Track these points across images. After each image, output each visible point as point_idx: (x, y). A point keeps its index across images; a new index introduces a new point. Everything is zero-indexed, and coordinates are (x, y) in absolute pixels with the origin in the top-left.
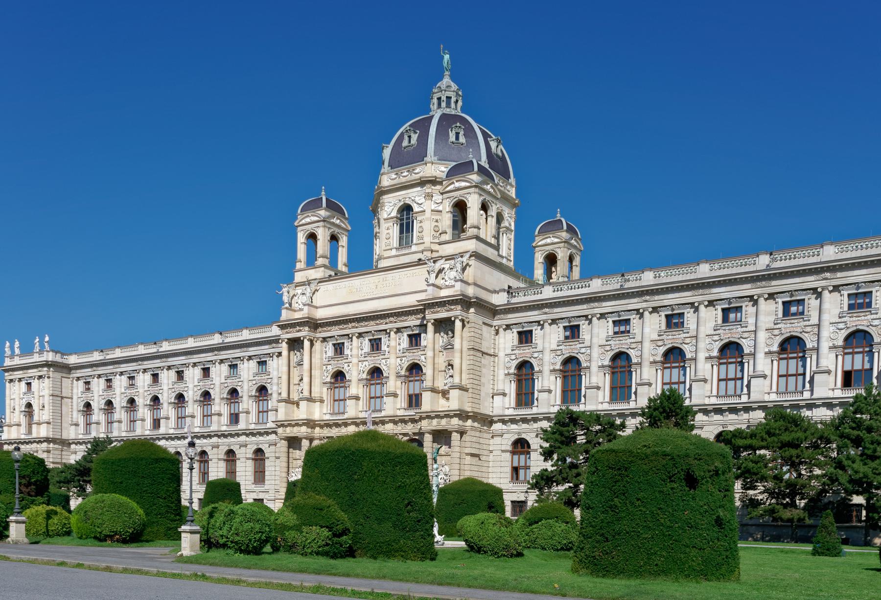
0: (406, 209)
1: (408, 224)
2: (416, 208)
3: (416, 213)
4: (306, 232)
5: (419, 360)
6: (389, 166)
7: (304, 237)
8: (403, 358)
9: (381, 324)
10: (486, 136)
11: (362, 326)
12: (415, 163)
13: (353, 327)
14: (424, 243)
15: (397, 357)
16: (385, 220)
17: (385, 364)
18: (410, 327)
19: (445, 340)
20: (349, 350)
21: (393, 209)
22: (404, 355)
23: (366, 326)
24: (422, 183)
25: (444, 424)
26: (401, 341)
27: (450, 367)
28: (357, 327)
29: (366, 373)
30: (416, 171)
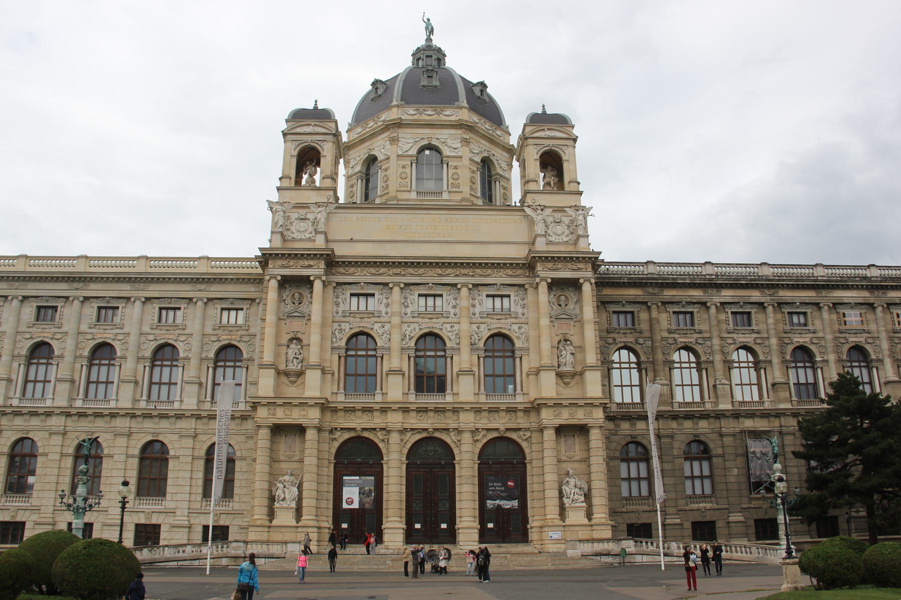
2: (446, 152)
3: (448, 157)
4: (301, 144)
6: (401, 100)
8: (482, 326)
11: (412, 275)
14: (461, 192)
15: (471, 323)
16: (398, 156)
17: (449, 329)
18: (496, 284)
19: (555, 308)
21: (411, 147)
22: (483, 320)
23: (419, 275)
24: (460, 125)
25: (580, 417)
26: (476, 302)
28: (404, 275)
30: (445, 113)
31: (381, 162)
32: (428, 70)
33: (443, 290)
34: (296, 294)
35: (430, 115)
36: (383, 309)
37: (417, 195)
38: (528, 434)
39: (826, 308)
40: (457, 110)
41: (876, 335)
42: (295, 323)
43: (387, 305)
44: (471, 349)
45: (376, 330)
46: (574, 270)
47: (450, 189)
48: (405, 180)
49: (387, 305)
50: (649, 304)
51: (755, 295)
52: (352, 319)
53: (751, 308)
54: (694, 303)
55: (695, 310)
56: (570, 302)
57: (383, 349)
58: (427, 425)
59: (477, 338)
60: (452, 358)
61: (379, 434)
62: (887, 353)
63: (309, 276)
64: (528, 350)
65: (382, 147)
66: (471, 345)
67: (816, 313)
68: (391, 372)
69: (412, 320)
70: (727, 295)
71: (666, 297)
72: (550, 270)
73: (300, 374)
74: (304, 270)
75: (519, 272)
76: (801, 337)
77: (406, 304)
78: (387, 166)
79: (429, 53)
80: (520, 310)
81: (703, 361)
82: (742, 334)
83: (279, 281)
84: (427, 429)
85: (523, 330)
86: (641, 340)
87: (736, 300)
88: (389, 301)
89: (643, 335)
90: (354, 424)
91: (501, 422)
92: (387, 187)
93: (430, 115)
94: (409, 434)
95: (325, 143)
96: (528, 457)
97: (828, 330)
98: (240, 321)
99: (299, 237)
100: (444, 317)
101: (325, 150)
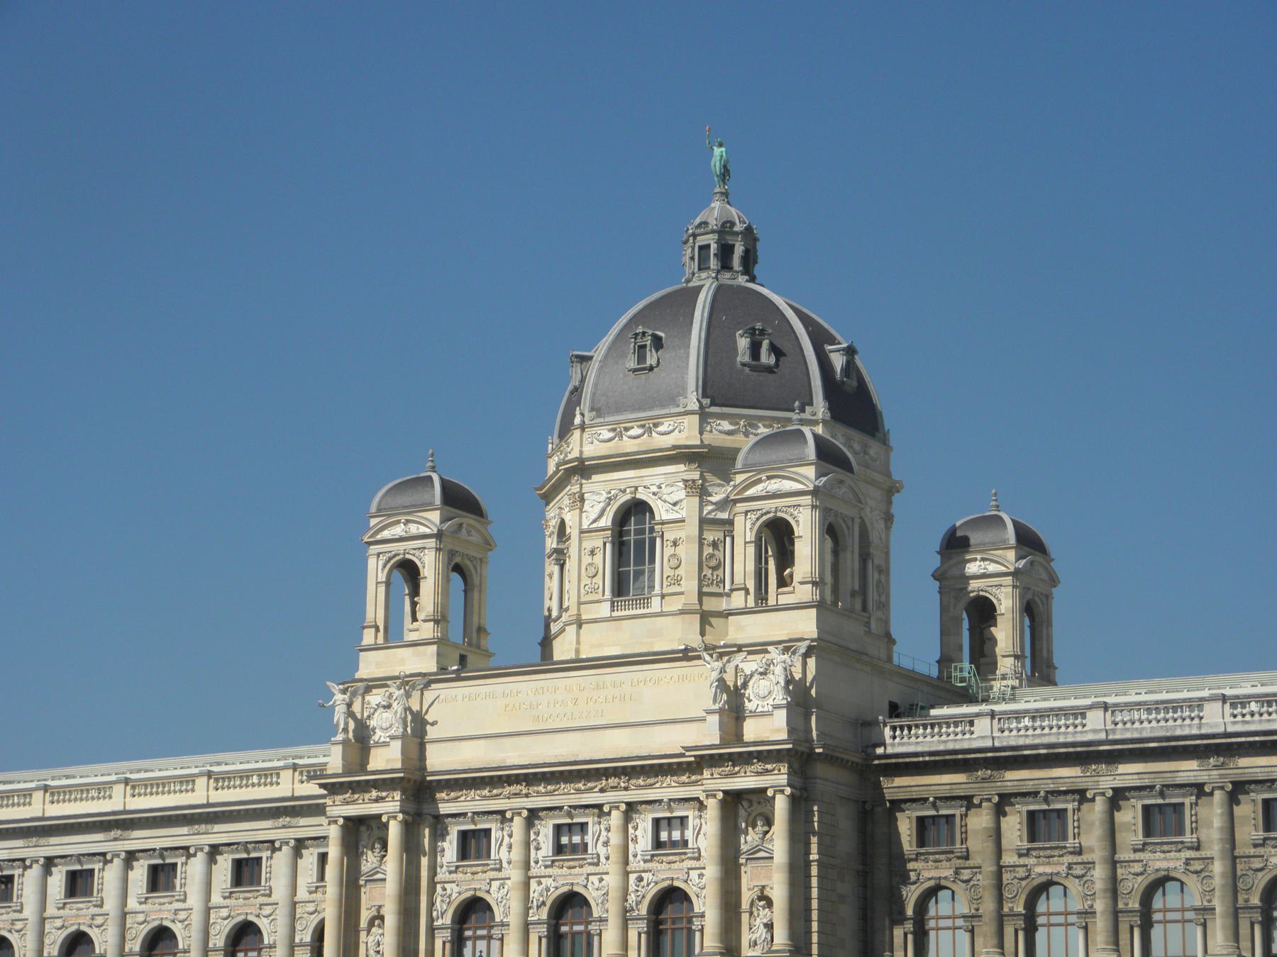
0: (634, 511)
1: (640, 545)
2: (662, 512)
3: (663, 523)
4: (390, 559)
5: (686, 881)
9: (590, 790)
10: (820, 338)
13: (517, 795)
14: (682, 593)
20: (504, 849)
26: (639, 833)
27: (762, 903)
28: (527, 796)
32: (637, 334)
35: (635, 438)
37: (612, 606)
40: (679, 419)
43: (510, 847)
46: (759, 774)
47: (665, 591)
48: (594, 580)
51: (1188, 770)
52: (459, 876)
53: (1184, 796)
55: (1070, 806)
59: (634, 899)
63: (379, 816)
66: (625, 911)
69: (543, 871)
70: (1129, 773)
71: (1009, 784)
79: (702, 240)
82: (1164, 852)
86: (966, 871)
87: (1146, 782)
89: (971, 863)
93: (635, 438)
95: (426, 551)
100: (590, 864)
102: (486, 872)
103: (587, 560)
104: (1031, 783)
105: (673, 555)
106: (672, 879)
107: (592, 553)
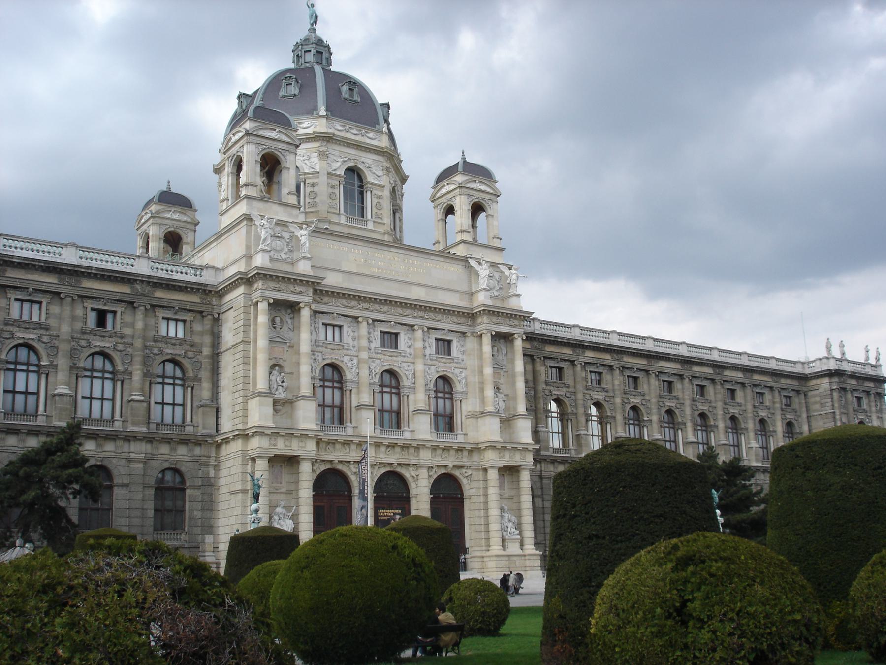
0: (354, 172)
2: (370, 178)
3: (373, 184)
4: (265, 149)
7: (261, 155)
8: (433, 367)
12: (352, 121)
14: (384, 224)
15: (425, 364)
16: (328, 173)
17: (406, 369)
18: (444, 329)
23: (384, 313)
28: (372, 311)
29: (378, 376)
30: (368, 135)
31: (305, 174)
32: (351, 82)
33: (401, 330)
34: (278, 320)
35: (356, 135)
36: (351, 342)
38: (469, 472)
39: (653, 375)
41: (682, 402)
42: (276, 348)
44: (426, 390)
45: (347, 363)
47: (374, 219)
49: (354, 339)
50: (535, 357)
51: (607, 358)
52: (323, 349)
54: (565, 360)
55: (565, 367)
56: (500, 353)
57: (352, 382)
58: (393, 460)
60: (408, 396)
61: (352, 467)
62: (689, 417)
64: (467, 394)
65: (306, 157)
67: (645, 379)
68: (360, 407)
72: (494, 323)
73: (290, 403)
74: (295, 296)
75: (462, 320)
76: (635, 398)
77: (370, 339)
78: (314, 181)
80: (461, 356)
81: (570, 413)
83: (270, 304)
84: (392, 464)
85: (463, 375)
87: (595, 361)
88: (356, 334)
90: (334, 457)
91: (449, 461)
92: (315, 205)
93: (356, 135)
94: (376, 468)
95: (288, 153)
96: (466, 493)
97: (653, 395)
98: (180, 335)
99: (275, 257)
101: (288, 161)
102: (340, 350)
103: (331, 190)
104: (555, 354)
105: (379, 203)
106: (447, 371)
107: (333, 187)
